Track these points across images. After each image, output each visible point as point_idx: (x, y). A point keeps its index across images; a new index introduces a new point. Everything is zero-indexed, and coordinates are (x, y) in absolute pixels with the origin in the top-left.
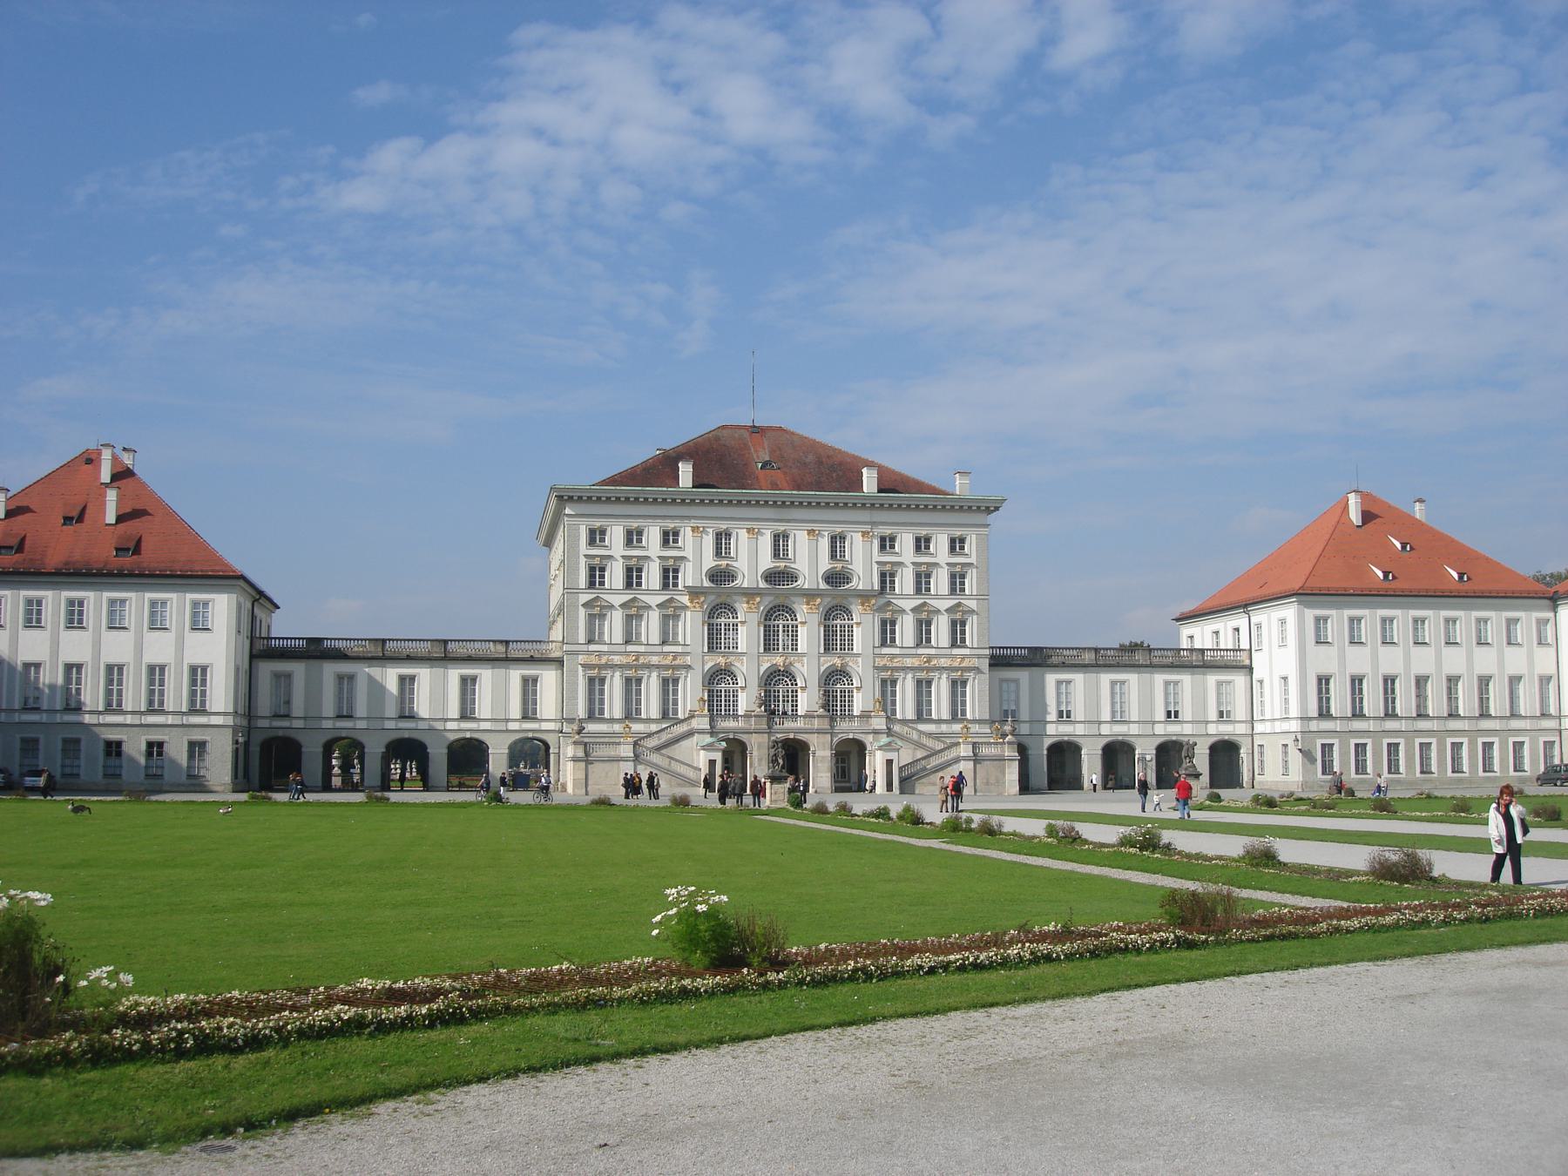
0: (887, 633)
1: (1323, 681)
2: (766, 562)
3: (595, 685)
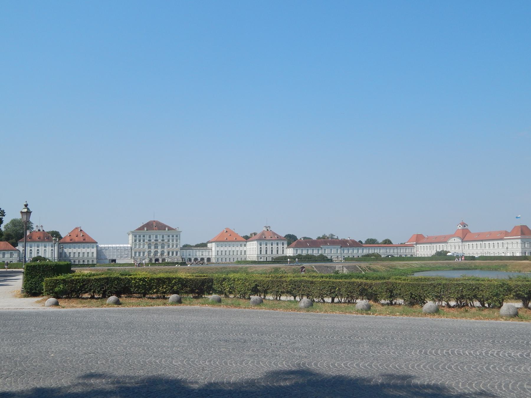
0: (169, 246)
1: (218, 251)
2: (155, 239)
3: (135, 253)
